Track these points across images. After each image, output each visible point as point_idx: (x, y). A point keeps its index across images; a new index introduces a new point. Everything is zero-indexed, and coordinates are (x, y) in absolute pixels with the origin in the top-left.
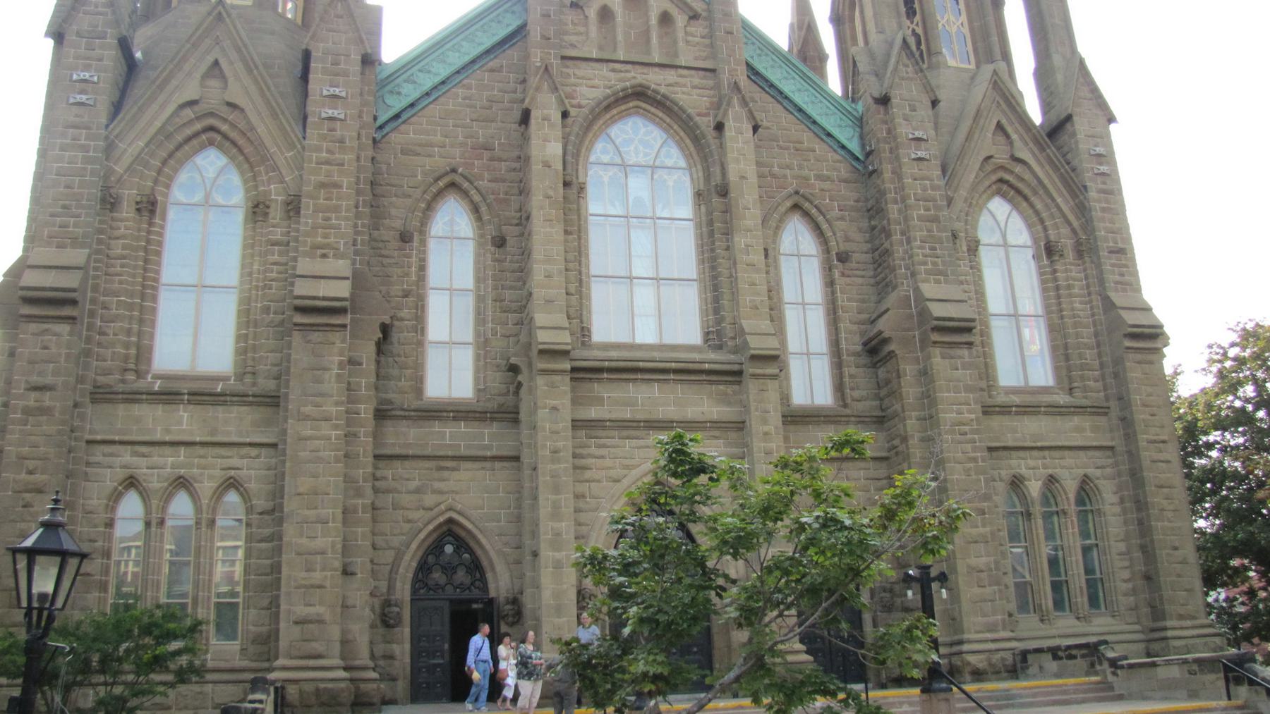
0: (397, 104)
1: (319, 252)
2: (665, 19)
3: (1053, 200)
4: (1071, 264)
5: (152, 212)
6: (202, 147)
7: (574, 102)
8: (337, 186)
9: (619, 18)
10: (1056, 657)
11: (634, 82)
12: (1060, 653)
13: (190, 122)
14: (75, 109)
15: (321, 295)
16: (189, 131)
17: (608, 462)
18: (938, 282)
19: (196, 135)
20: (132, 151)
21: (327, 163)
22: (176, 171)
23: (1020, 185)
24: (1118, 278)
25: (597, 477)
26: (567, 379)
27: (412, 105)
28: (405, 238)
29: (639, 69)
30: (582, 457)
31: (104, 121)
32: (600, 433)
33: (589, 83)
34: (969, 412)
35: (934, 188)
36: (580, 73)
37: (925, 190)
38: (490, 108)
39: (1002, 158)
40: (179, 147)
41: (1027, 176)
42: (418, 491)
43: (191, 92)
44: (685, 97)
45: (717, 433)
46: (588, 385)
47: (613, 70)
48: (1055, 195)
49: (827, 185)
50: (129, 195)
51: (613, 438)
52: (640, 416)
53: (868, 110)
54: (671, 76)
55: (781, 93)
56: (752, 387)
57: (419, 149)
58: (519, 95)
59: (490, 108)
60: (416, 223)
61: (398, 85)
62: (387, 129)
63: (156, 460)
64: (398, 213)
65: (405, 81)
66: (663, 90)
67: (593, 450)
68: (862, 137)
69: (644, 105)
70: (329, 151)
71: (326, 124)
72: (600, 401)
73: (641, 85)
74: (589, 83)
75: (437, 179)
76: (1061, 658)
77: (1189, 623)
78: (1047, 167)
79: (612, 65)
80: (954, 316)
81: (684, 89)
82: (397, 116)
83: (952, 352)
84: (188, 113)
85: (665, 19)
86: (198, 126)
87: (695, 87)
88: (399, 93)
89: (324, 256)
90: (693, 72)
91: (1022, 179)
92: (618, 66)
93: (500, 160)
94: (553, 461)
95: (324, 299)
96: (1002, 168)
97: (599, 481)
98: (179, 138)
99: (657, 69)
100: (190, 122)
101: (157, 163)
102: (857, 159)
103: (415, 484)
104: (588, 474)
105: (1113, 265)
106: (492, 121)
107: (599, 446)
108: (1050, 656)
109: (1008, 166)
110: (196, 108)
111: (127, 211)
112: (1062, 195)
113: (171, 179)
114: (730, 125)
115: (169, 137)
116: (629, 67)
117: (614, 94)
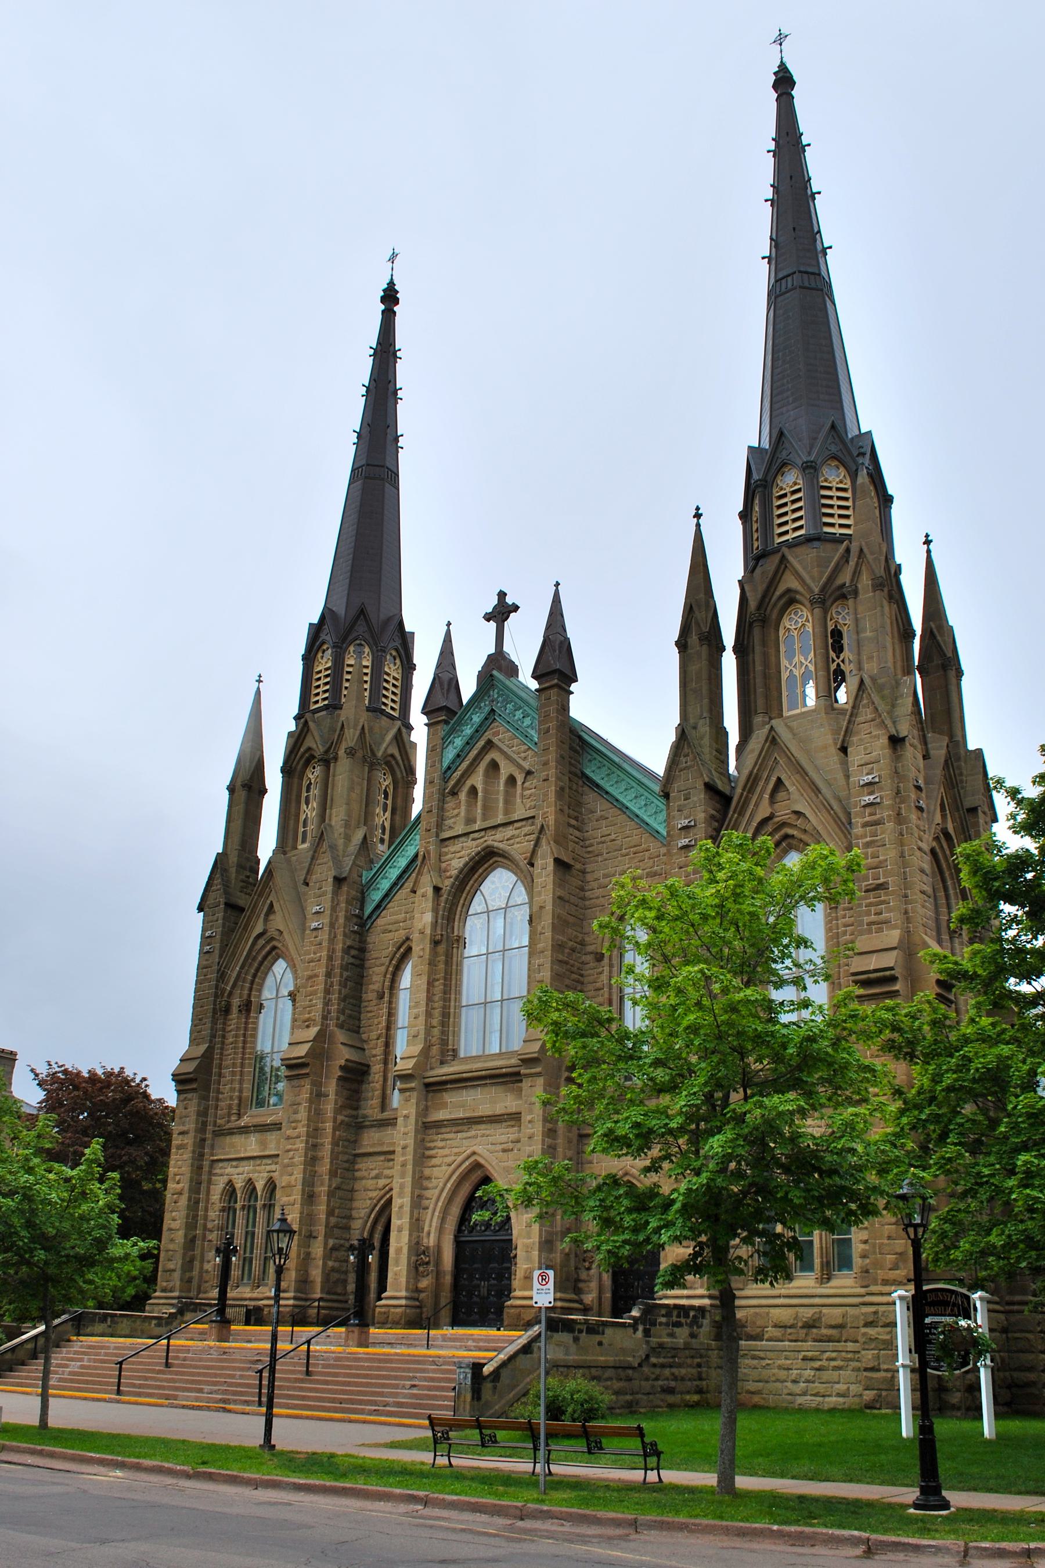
0: (376, 896)
2: (511, 780)
4: (844, 909)
5: (248, 1011)
7: (448, 874)
8: (316, 976)
9: (480, 794)
13: (264, 946)
16: (264, 953)
17: (446, 1151)
19: (269, 953)
20: (235, 974)
21: (312, 961)
22: (264, 979)
24: (873, 918)
25: (438, 1163)
27: (386, 895)
28: (381, 996)
29: (490, 832)
30: (430, 1149)
31: (217, 960)
32: (443, 1130)
33: (458, 855)
36: (452, 849)
39: (783, 813)
40: (261, 963)
42: (377, 1177)
43: (259, 929)
45: (512, 1123)
46: (439, 1095)
47: (473, 840)
50: (236, 1002)
54: (509, 831)
55: (623, 805)
56: (526, 1084)
57: (390, 927)
60: (387, 984)
62: (374, 917)
63: (240, 1170)
64: (377, 976)
67: (441, 1144)
71: (315, 933)
72: (444, 1106)
73: (488, 847)
74: (458, 855)
75: (399, 948)
79: (472, 836)
81: (518, 840)
82: (378, 906)
84: (261, 942)
85: (511, 780)
86: (268, 948)
87: (525, 835)
90: (524, 823)
92: (476, 835)
96: (784, 824)
97: (440, 1166)
98: (260, 958)
99: (500, 829)
100: (264, 946)
101: (249, 978)
103: (374, 1173)
104: (434, 1161)
105: (868, 905)
107: (442, 1140)
109: (789, 821)
110: (265, 937)
111: (234, 1014)
113: (262, 985)
114: (539, 862)
115: (255, 959)
116: (483, 833)
117: (471, 860)
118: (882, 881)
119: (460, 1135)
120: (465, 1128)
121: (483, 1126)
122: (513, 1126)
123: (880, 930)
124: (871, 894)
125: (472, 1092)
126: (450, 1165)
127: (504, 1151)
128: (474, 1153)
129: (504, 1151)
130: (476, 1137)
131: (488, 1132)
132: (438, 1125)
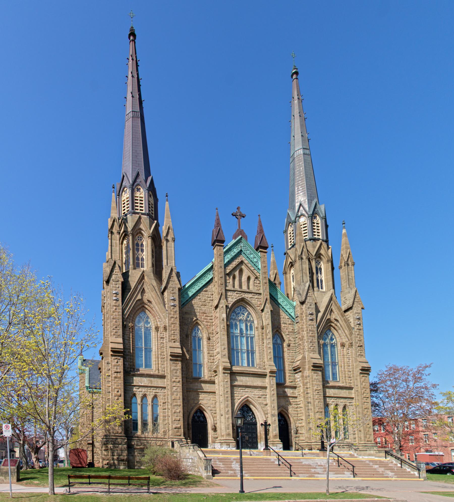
1: (173, 341)
3: (344, 331)
6: (141, 312)
10: (339, 447)
11: (242, 297)
12: (340, 447)
14: (114, 301)
15: (176, 352)
16: (139, 307)
18: (314, 353)
19: (140, 308)
23: (336, 327)
26: (229, 375)
27: (187, 301)
34: (320, 387)
35: (314, 328)
37: (312, 328)
38: (205, 302)
41: (338, 324)
44: (254, 301)
48: (345, 330)
49: (285, 325)
51: (238, 389)
52: (244, 384)
53: (297, 305)
58: (211, 299)
59: (205, 302)
61: (184, 295)
65: (185, 294)
66: (249, 299)
68: (294, 312)
69: (243, 303)
70: (173, 315)
76: (340, 448)
77: (369, 443)
78: (344, 322)
80: (318, 363)
82: (184, 304)
83: (316, 372)
86: (141, 306)
88: (184, 297)
89: (174, 342)
91: (336, 325)
93: (208, 316)
94: (227, 394)
95: (177, 353)
102: (293, 318)
106: (206, 306)
108: (338, 447)
112: (346, 328)
118: (361, 345)
119: (242, 391)
120: (244, 388)
121: (250, 389)
122: (261, 390)
123: (361, 357)
124: (359, 347)
125: (244, 377)
126: (239, 399)
127: (259, 397)
128: (248, 397)
129: (259, 397)
130: (248, 392)
131: (252, 391)
132: (236, 386)
